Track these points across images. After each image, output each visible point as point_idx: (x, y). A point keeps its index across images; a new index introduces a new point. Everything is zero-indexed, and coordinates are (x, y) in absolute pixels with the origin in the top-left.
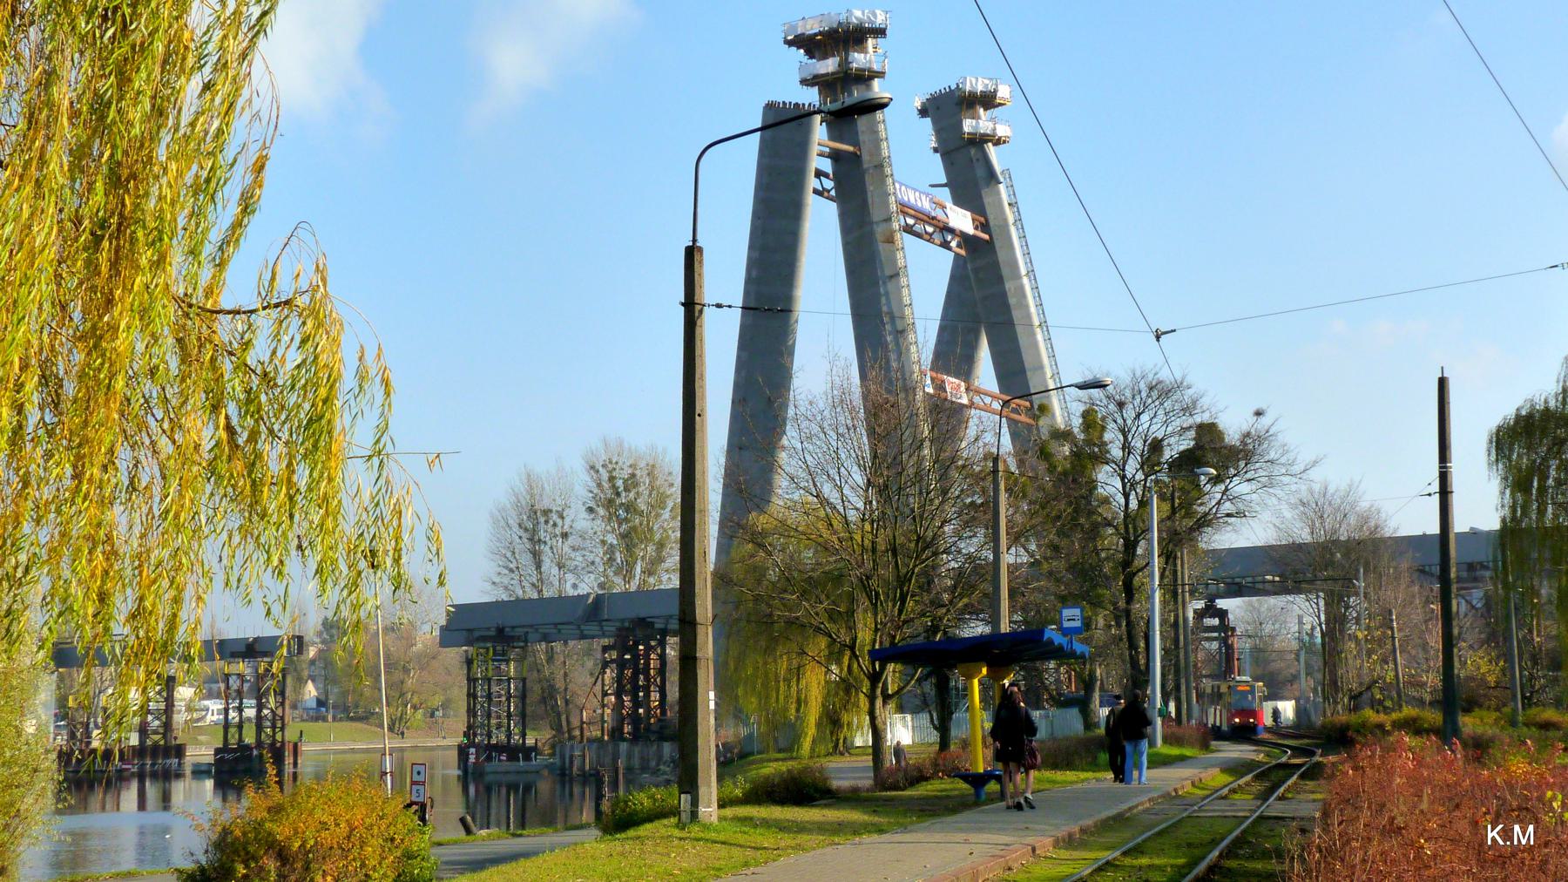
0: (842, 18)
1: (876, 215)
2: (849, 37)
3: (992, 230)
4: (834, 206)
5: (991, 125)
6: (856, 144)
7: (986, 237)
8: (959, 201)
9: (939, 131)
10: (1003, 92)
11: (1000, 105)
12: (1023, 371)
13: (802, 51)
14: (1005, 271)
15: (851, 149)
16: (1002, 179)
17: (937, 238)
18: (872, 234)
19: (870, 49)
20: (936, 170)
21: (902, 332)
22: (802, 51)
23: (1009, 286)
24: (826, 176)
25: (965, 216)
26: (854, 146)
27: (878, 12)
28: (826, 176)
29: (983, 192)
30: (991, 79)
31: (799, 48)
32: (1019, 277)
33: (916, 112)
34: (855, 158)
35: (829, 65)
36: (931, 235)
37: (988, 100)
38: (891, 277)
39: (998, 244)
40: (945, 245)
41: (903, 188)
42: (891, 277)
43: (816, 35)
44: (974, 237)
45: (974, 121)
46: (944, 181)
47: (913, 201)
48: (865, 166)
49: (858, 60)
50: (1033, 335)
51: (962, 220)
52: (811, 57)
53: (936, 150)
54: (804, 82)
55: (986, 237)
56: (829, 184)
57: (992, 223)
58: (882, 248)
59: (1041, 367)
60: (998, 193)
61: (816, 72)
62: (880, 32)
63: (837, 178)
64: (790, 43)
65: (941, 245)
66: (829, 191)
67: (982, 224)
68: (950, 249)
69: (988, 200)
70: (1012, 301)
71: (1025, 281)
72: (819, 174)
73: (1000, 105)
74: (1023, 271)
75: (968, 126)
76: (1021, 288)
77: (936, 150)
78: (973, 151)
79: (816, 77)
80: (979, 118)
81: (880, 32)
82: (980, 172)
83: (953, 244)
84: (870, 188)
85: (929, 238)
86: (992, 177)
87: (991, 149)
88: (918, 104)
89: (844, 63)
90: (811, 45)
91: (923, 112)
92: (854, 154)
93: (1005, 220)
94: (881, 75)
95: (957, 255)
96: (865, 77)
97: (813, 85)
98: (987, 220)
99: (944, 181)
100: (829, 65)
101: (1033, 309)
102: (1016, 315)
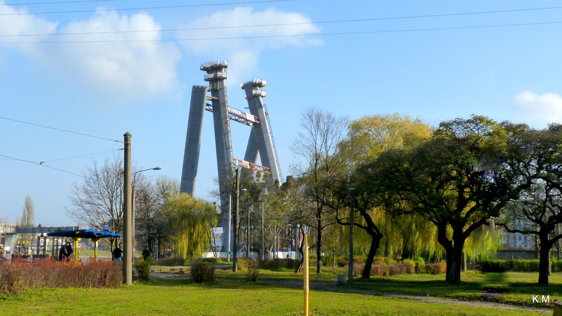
0: (216, 63)
1: (223, 116)
2: (218, 68)
4: (212, 113)
5: (260, 92)
6: (218, 97)
7: (259, 122)
8: (252, 113)
9: (247, 93)
10: (264, 83)
11: (264, 86)
12: (268, 160)
13: (206, 72)
14: (264, 132)
15: (216, 98)
16: (263, 106)
17: (245, 122)
18: (221, 122)
19: (223, 71)
20: (246, 104)
21: (229, 148)
22: (206, 72)
23: (265, 136)
24: (211, 105)
25: (252, 116)
26: (217, 97)
27: (225, 61)
28: (211, 105)
29: (258, 111)
30: (261, 79)
31: (205, 71)
32: (268, 134)
34: (218, 101)
35: (212, 76)
36: (243, 122)
37: (260, 85)
38: (226, 133)
40: (248, 124)
41: (233, 109)
42: (226, 133)
43: (208, 67)
44: (255, 122)
45: (256, 91)
46: (248, 107)
47: (235, 112)
48: (220, 103)
49: (219, 74)
50: (271, 149)
51: (251, 118)
52: (208, 73)
53: (246, 98)
54: (205, 80)
55: (259, 122)
56: (211, 108)
57: (260, 118)
58: (224, 125)
59: (273, 158)
60: (262, 110)
61: (208, 77)
62: (226, 67)
63: (214, 106)
64: (202, 70)
65: (246, 124)
66: (211, 110)
67: (257, 119)
68: (249, 125)
69: (259, 112)
70: (265, 140)
71: (269, 134)
72: (208, 105)
73: (264, 86)
74: (269, 132)
76: (268, 136)
77: (246, 98)
78: (256, 99)
79: (208, 79)
80: (258, 90)
81: (226, 67)
82: (257, 105)
83: (250, 124)
84: (221, 109)
85: (243, 122)
86: (261, 106)
87: (261, 99)
88: (242, 86)
89: (216, 75)
90: (209, 70)
91: (243, 88)
92: (217, 100)
93: (264, 118)
94: (226, 78)
95: (252, 127)
96: (221, 79)
97: (208, 81)
98: (259, 118)
99: (248, 107)
100: (212, 76)
101: (271, 142)
102: (267, 144)
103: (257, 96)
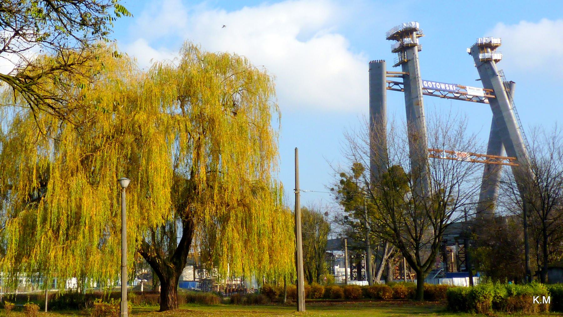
2: (409, 32)
3: (496, 93)
7: (493, 96)
16: (498, 74)
23: (504, 114)
33: (468, 54)
39: (498, 99)
46: (480, 78)
55: (493, 96)
60: (498, 79)
68: (484, 103)
69: (493, 83)
70: (506, 119)
71: (511, 111)
75: (481, 56)
82: (490, 72)
86: (494, 74)
88: (469, 50)
98: (493, 90)
101: (515, 122)
103: (488, 61)
